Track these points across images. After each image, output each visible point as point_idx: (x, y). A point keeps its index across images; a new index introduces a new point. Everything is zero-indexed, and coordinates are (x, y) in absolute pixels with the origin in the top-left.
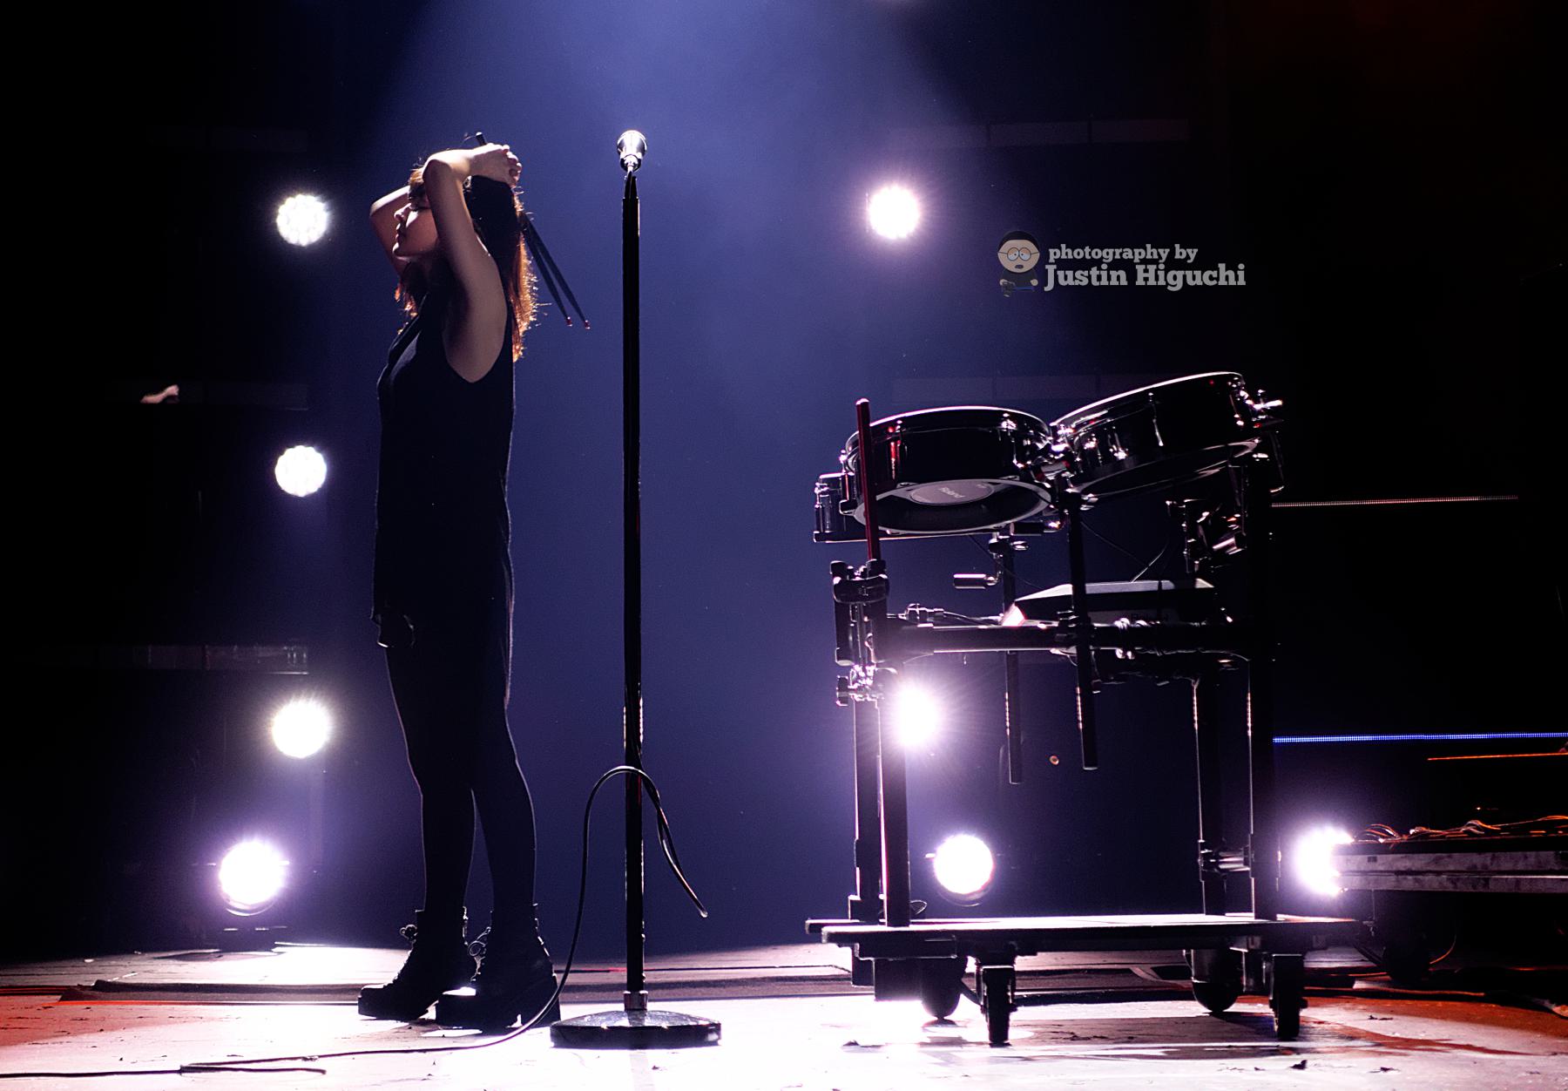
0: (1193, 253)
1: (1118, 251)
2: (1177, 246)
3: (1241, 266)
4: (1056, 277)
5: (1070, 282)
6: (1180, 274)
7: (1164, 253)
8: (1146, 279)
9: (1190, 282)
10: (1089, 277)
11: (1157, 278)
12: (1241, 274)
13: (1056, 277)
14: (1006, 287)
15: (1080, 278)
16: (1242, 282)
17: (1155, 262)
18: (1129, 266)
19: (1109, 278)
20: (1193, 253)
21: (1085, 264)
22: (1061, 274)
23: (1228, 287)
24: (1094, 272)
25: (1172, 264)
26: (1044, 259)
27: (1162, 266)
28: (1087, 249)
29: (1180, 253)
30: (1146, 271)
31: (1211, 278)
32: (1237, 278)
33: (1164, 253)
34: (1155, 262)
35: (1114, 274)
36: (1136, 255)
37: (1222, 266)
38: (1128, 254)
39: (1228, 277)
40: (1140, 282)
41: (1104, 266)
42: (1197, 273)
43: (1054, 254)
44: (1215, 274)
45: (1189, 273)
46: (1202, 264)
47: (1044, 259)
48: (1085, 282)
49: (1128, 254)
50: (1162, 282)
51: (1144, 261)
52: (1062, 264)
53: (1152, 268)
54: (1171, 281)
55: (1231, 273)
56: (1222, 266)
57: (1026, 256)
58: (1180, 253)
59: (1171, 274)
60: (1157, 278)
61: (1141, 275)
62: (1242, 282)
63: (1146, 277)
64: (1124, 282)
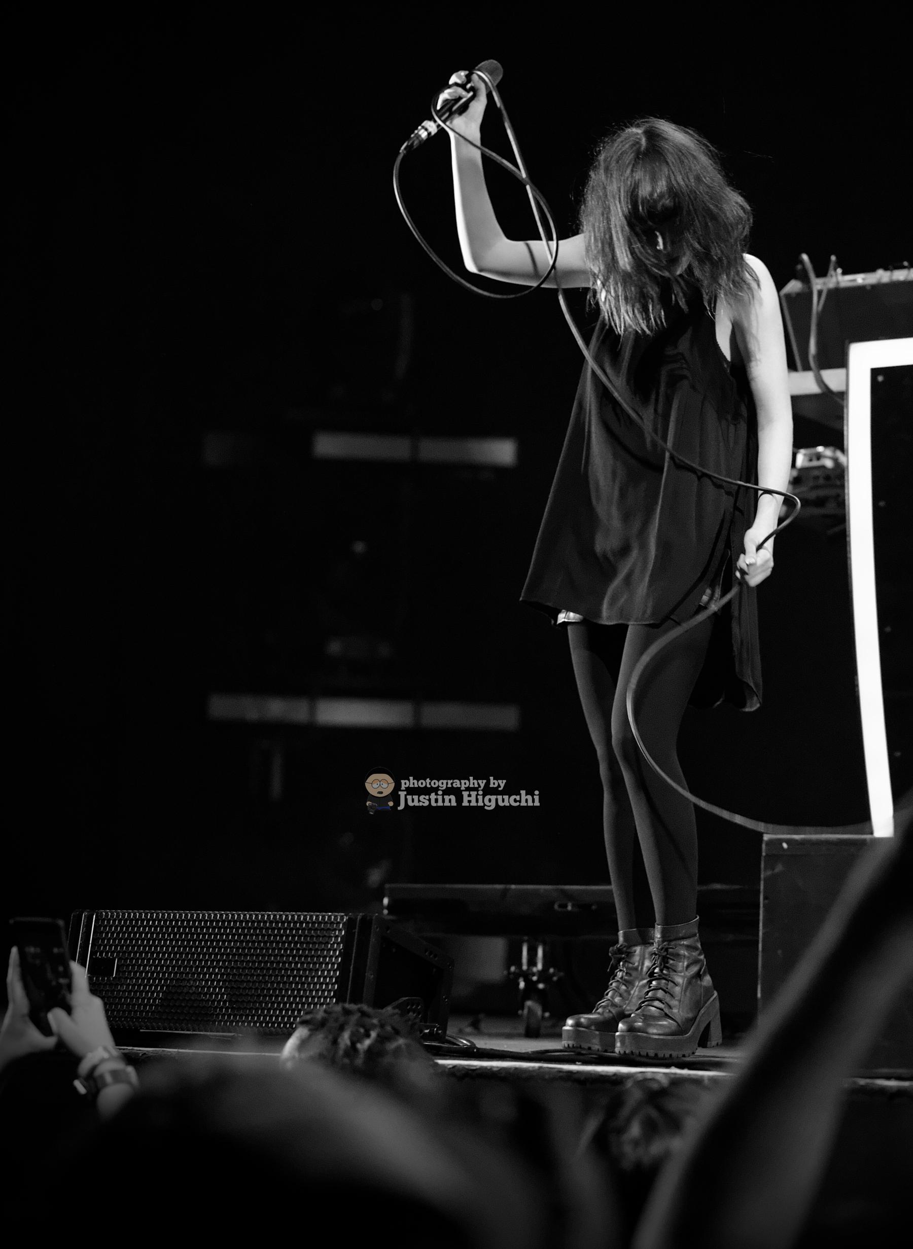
0: (502, 783)
1: (450, 782)
2: (492, 778)
3: (537, 792)
4: (406, 800)
5: (416, 803)
6: (493, 798)
7: (482, 783)
8: (469, 802)
9: (501, 804)
10: (429, 800)
11: (477, 801)
12: (537, 798)
13: (406, 800)
14: (371, 807)
15: (422, 801)
16: (537, 804)
17: (476, 789)
18: (457, 793)
19: (443, 801)
20: (502, 783)
21: (427, 791)
22: (409, 797)
23: (527, 807)
24: (433, 796)
25: (488, 791)
26: (398, 787)
27: (481, 793)
28: (428, 780)
29: (493, 783)
30: (469, 796)
31: (515, 801)
32: (533, 801)
33: (482, 783)
34: (476, 789)
35: (447, 798)
36: (463, 784)
37: (523, 792)
38: (457, 784)
39: (528, 800)
40: (465, 803)
41: (440, 792)
42: (506, 797)
43: (404, 784)
44: (518, 798)
45: (500, 797)
46: (508, 791)
47: (398, 787)
48: (427, 803)
49: (457, 784)
50: (480, 804)
51: (468, 789)
52: (410, 791)
53: (474, 793)
54: (487, 802)
55: (529, 797)
56: (523, 792)
57: (385, 785)
58: (493, 783)
59: (487, 797)
60: (477, 801)
61: (466, 799)
62: (537, 804)
63: (468, 800)
64: (454, 804)
